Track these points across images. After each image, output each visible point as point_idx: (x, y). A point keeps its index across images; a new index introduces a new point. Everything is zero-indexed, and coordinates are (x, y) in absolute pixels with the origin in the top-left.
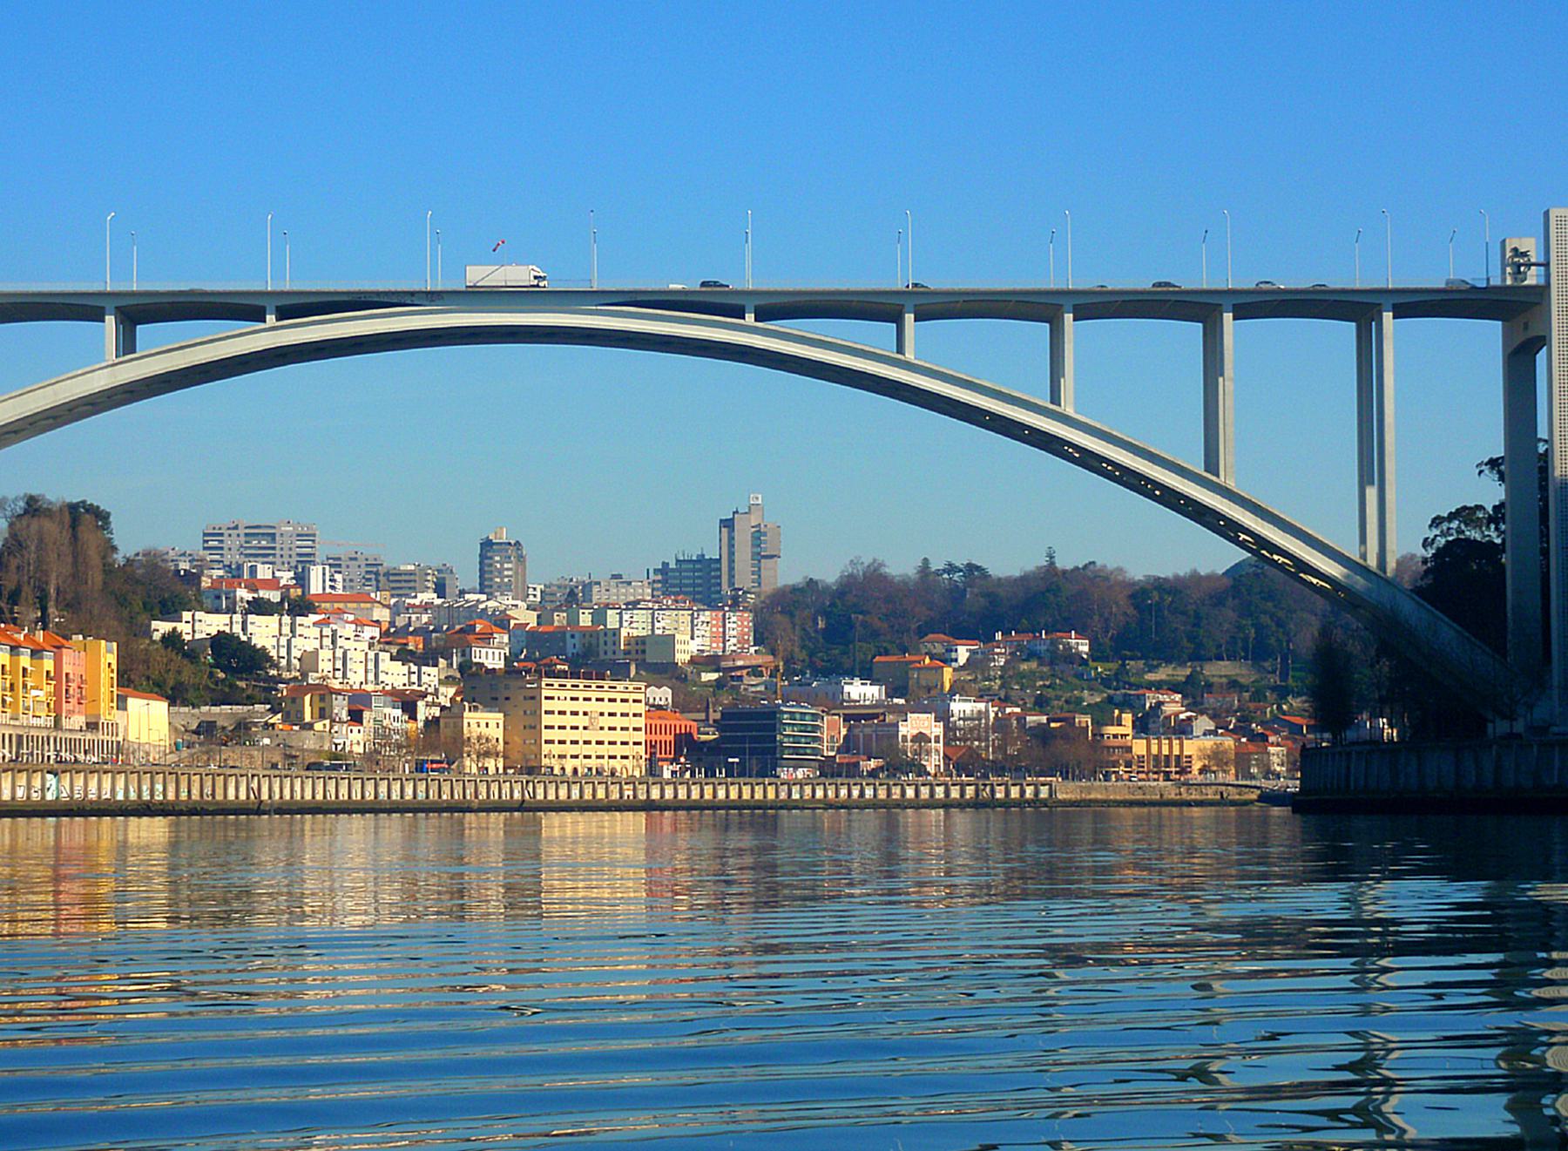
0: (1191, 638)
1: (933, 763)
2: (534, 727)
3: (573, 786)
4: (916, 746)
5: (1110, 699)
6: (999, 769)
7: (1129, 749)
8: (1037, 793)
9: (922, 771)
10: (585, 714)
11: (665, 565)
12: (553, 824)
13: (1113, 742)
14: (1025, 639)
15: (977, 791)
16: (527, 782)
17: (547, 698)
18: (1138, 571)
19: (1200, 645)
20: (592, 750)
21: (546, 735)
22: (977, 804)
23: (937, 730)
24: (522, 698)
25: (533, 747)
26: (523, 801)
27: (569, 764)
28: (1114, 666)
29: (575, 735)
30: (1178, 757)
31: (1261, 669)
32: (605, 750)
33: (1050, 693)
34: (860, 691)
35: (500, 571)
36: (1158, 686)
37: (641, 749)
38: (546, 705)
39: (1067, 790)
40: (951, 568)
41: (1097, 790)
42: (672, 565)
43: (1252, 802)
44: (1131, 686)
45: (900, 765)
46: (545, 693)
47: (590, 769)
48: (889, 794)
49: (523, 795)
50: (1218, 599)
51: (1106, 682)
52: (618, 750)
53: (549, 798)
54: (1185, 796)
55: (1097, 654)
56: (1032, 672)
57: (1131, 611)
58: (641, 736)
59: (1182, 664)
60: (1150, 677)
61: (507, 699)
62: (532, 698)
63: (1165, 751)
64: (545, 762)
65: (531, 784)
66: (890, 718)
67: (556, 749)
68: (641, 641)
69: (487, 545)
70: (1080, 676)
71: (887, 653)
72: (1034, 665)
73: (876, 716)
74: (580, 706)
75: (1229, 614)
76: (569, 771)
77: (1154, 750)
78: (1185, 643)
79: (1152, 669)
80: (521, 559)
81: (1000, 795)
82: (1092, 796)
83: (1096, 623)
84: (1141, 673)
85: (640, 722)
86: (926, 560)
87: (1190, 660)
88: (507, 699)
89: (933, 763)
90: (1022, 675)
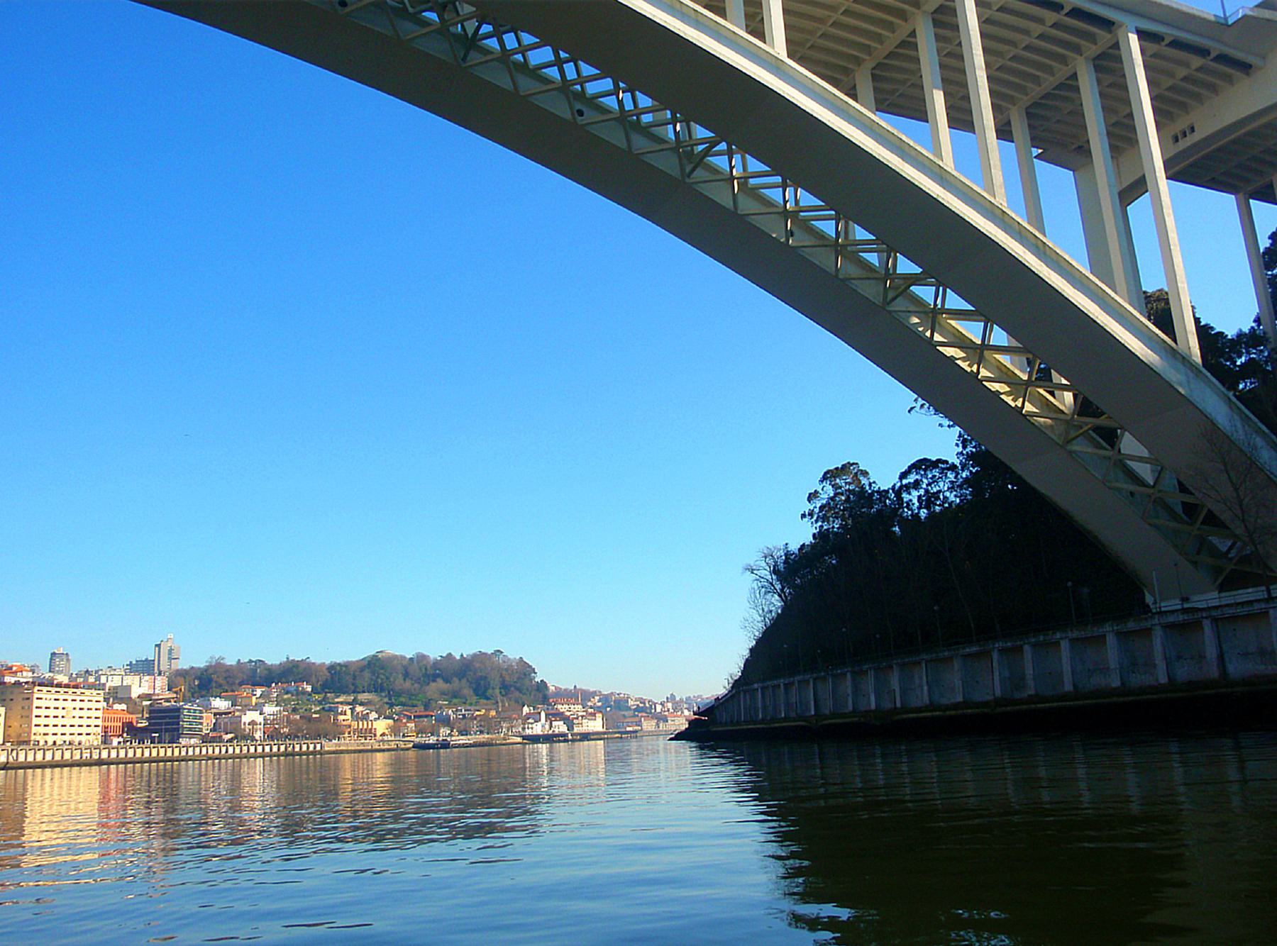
0: (353, 685)
1: (258, 735)
2: (27, 717)
3: (47, 752)
4: (251, 727)
5: (323, 708)
6: (292, 736)
7: (350, 726)
8: (315, 747)
9: (253, 739)
10: (63, 708)
11: (131, 662)
12: (34, 777)
13: (345, 723)
14: (285, 686)
15: (286, 749)
16: (12, 750)
17: (37, 699)
18: (328, 662)
19: (356, 687)
20: (68, 730)
21: (35, 721)
22: (286, 754)
23: (260, 719)
24: (21, 699)
25: (26, 729)
26: (8, 763)
27: (50, 739)
28: (322, 696)
29: (56, 721)
30: (371, 729)
31: (381, 696)
32: (76, 730)
33: (297, 706)
34: (220, 704)
35: (58, 666)
36: (341, 703)
37: (99, 730)
38: (36, 703)
39: (329, 746)
40: (251, 661)
41: (329, 746)
42: (134, 662)
43: (408, 749)
44: (330, 703)
45: (242, 737)
46: (36, 696)
47: (65, 742)
48: (301, 748)
49: (8, 759)
50: (362, 670)
51: (320, 703)
52: (84, 730)
53: (29, 760)
54: (382, 747)
55: (314, 691)
56: (289, 698)
57: (328, 674)
58: (99, 722)
59: (349, 694)
60: (336, 700)
61: (12, 700)
62: (28, 699)
63: (365, 727)
64: (33, 737)
65: (15, 752)
66: (237, 714)
67: (42, 730)
68: (115, 688)
69: (53, 654)
70: (308, 700)
71: (227, 691)
72: (289, 695)
73: (230, 713)
74: (60, 704)
75: (367, 674)
76: (50, 743)
77: (361, 727)
78: (350, 686)
79: (338, 697)
80: (68, 660)
81: (297, 749)
82: (341, 748)
83: (314, 679)
84: (333, 699)
85: (99, 714)
86: (239, 660)
87: (354, 692)
88: (12, 700)
89: (258, 735)
90: (284, 700)
